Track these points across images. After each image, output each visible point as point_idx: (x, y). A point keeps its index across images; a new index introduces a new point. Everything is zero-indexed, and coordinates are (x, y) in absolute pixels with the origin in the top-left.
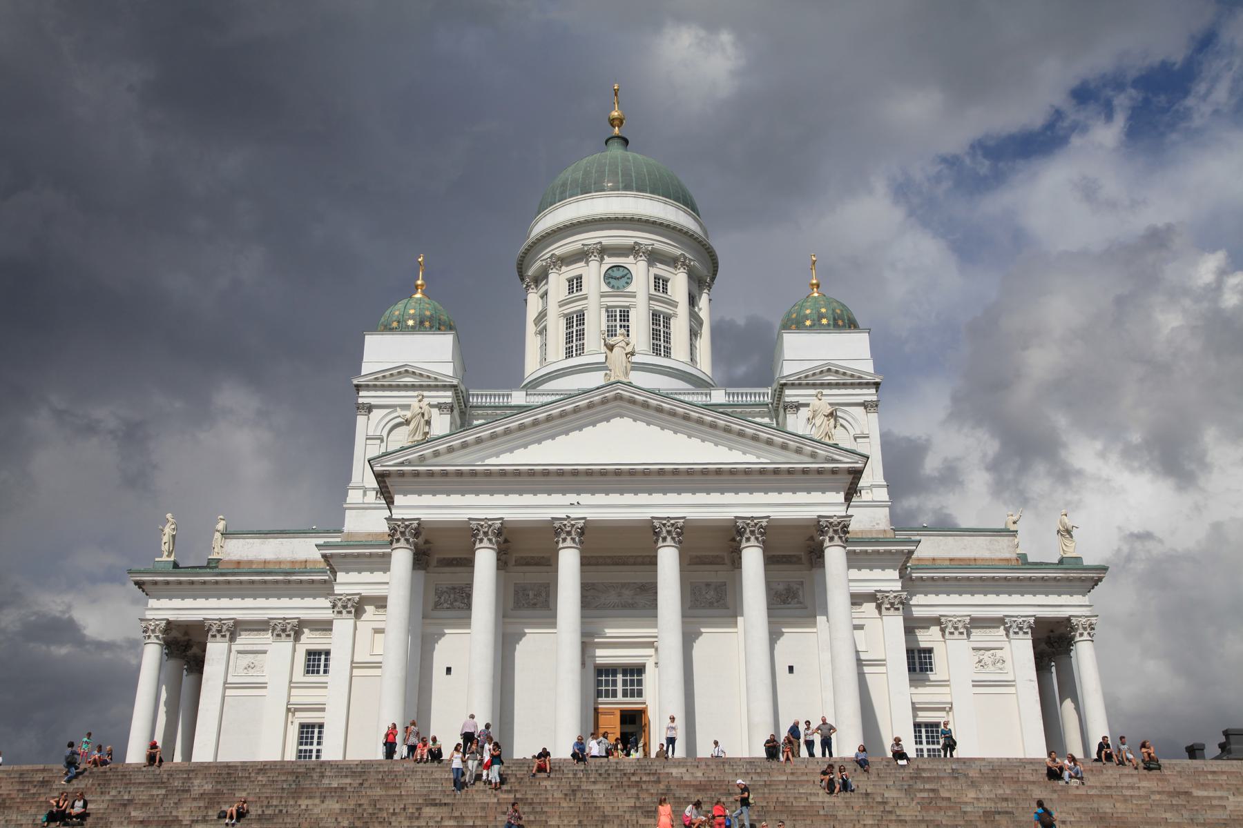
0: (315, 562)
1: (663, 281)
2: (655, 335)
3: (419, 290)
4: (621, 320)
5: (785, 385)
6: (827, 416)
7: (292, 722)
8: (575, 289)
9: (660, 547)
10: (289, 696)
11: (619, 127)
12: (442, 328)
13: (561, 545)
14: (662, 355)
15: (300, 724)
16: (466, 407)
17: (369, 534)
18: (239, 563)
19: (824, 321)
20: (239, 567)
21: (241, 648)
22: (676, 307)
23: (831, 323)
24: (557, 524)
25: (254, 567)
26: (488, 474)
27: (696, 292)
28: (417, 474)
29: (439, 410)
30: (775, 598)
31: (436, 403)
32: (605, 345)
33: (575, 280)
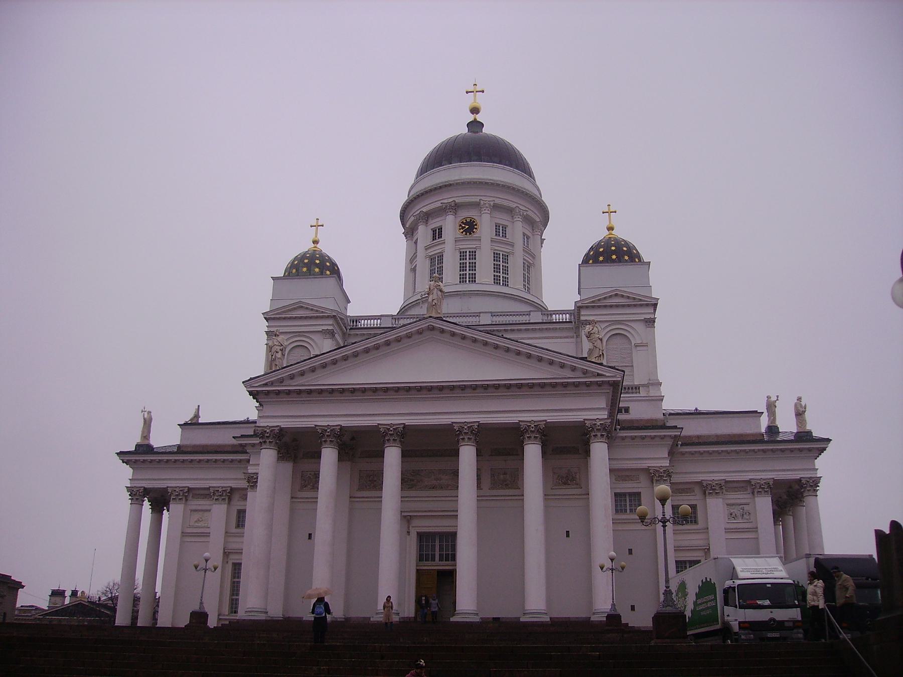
1: (502, 227)
2: (496, 268)
7: (227, 562)
10: (226, 542)
14: (501, 284)
15: (233, 563)
21: (194, 507)
22: (513, 246)
27: (529, 234)
28: (278, 393)
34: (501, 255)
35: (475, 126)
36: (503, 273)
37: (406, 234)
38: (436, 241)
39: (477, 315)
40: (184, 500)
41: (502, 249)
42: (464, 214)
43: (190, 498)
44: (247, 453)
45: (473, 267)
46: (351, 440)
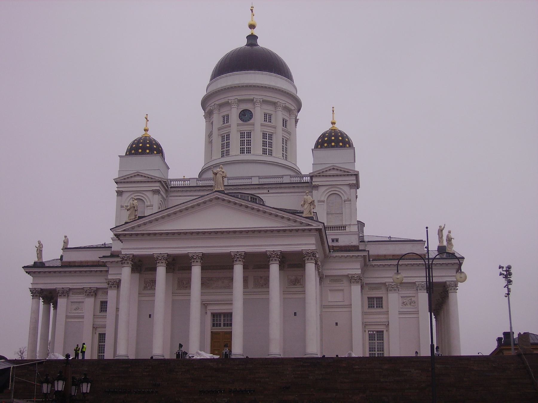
1: (269, 115)
2: (264, 144)
4: (247, 137)
5: (313, 176)
7: (95, 333)
9: (235, 264)
10: (94, 321)
12: (155, 152)
15: (99, 333)
16: (168, 188)
19: (333, 144)
22: (275, 128)
24: (190, 255)
25: (76, 264)
28: (131, 235)
30: (290, 283)
32: (213, 173)
34: (268, 134)
35: (252, 39)
36: (269, 146)
37: (205, 117)
39: (250, 178)
40: (66, 296)
41: (269, 130)
43: (71, 295)
44: (106, 266)
45: (249, 143)
46: (173, 261)
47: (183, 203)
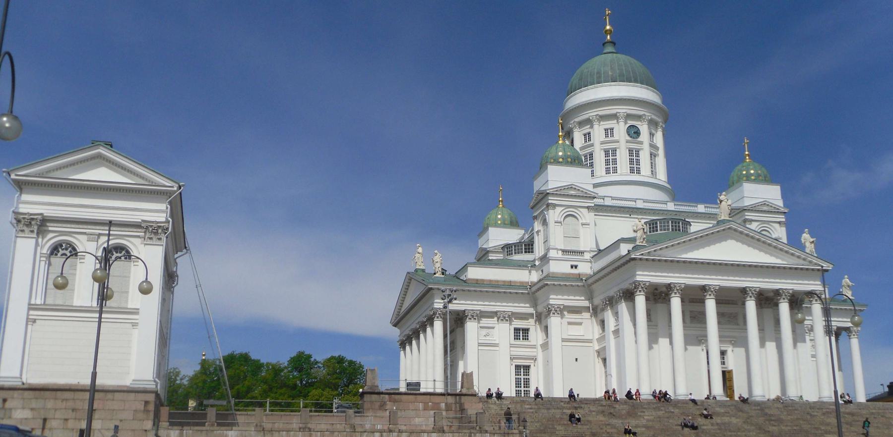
0: (515, 282)
3: (561, 139)
5: (746, 209)
6: (811, 242)
8: (609, 135)
11: (610, 34)
13: (708, 297)
17: (563, 274)
18: (477, 280)
20: (478, 282)
23: (763, 179)
24: (707, 288)
26: (678, 261)
28: (647, 260)
29: (588, 209)
31: (587, 206)
33: (609, 130)
38: (607, 139)
42: (630, 123)
47: (701, 230)
